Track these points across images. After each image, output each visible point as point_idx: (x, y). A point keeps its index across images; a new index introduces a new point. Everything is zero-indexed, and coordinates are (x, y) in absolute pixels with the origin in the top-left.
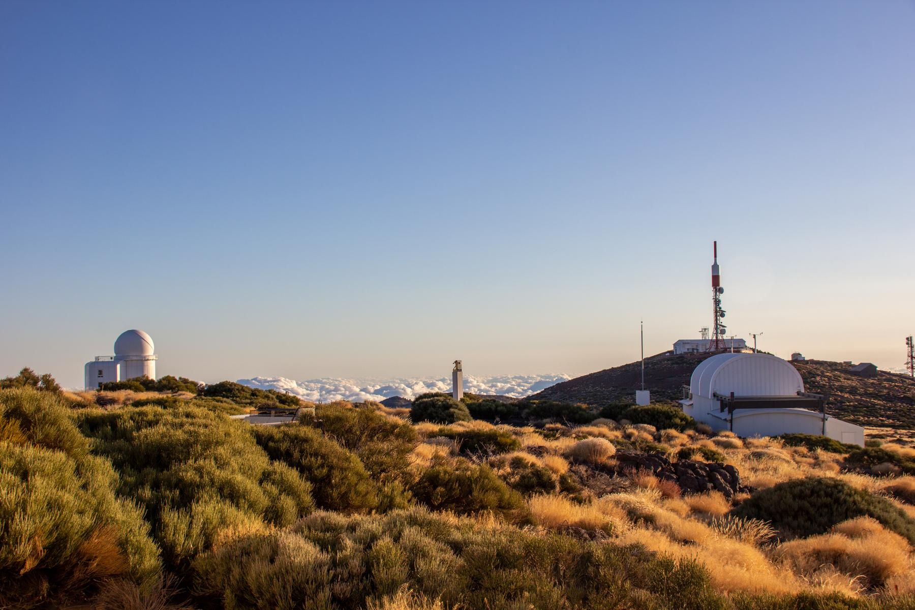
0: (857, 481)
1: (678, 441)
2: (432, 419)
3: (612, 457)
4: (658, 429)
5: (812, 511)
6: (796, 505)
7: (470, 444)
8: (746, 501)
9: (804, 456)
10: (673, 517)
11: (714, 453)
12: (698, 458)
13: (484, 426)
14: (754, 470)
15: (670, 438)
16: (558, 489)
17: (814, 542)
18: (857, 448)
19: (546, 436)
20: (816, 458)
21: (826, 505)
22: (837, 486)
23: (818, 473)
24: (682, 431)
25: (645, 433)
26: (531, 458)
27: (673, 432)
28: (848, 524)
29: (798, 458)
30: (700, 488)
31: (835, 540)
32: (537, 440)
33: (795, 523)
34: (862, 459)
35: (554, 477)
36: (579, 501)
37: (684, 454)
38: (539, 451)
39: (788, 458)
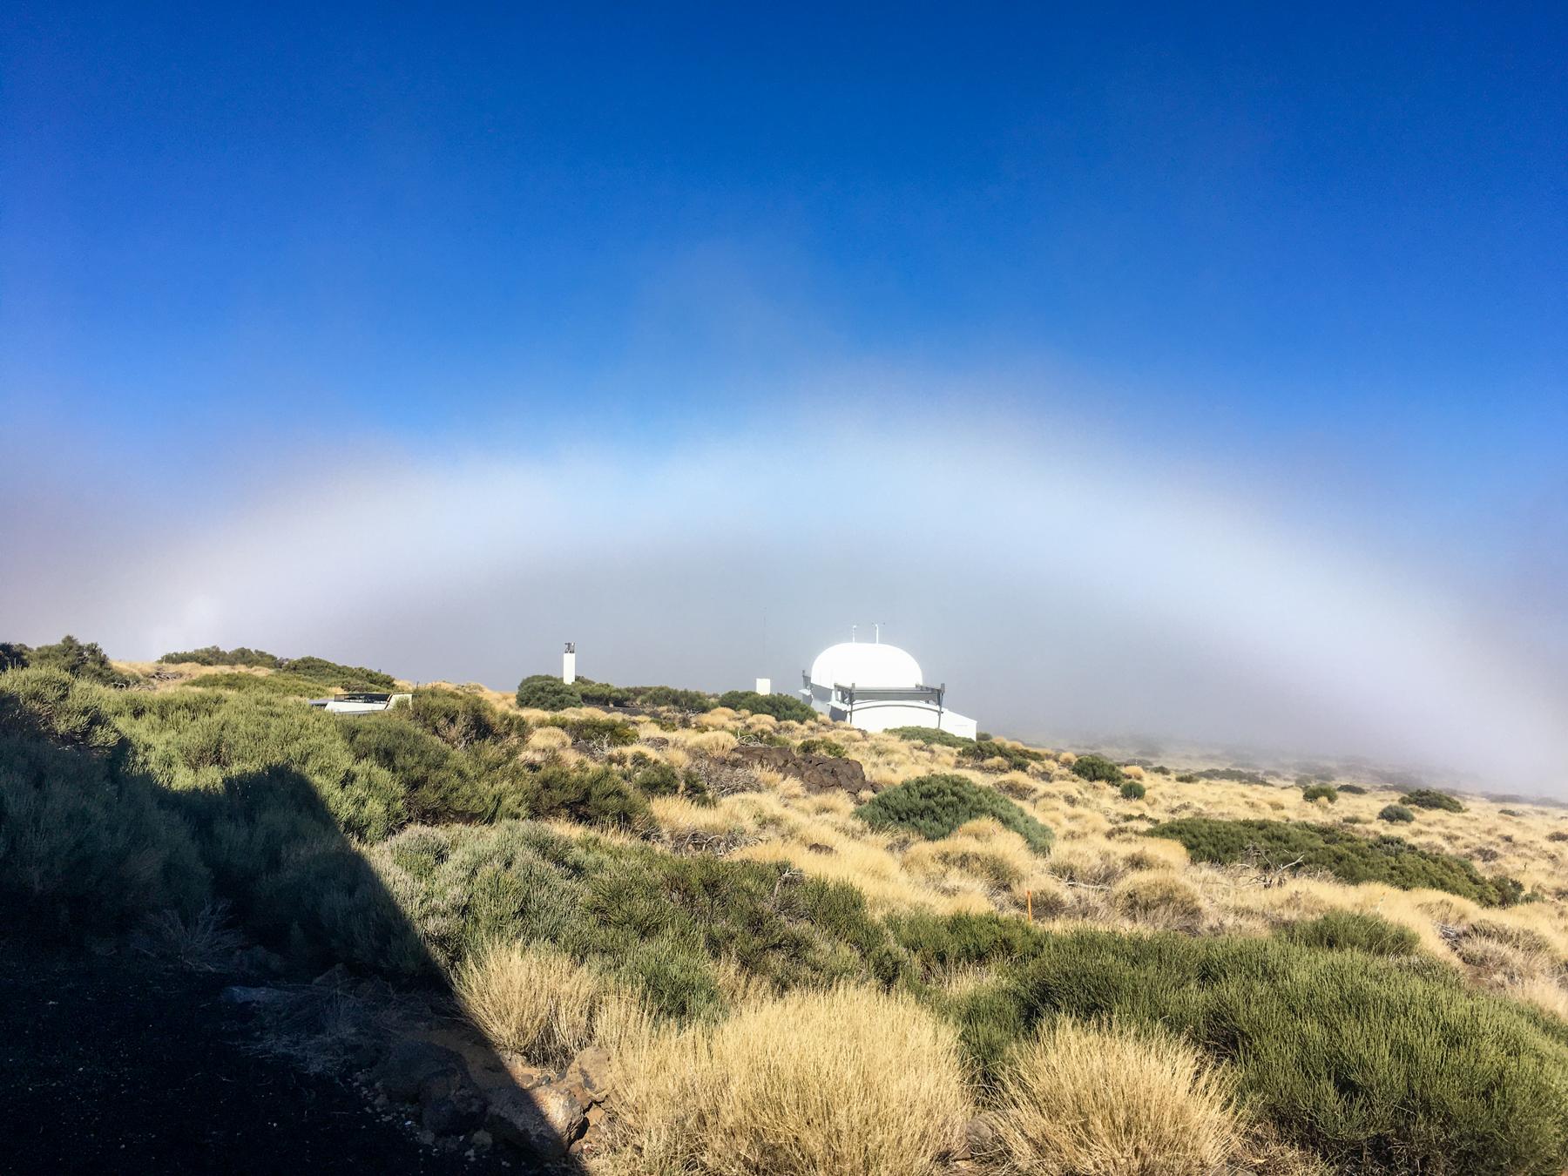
1: (797, 733)
2: (540, 704)
4: (778, 719)
5: (938, 810)
6: (922, 803)
7: (583, 734)
8: (872, 801)
9: (921, 749)
11: (837, 747)
12: (822, 752)
13: (599, 714)
14: (875, 765)
17: (942, 845)
18: (971, 741)
19: (663, 727)
20: (932, 752)
21: (952, 804)
22: (958, 782)
23: (938, 769)
24: (802, 722)
25: (766, 722)
26: (652, 754)
27: (793, 723)
28: (972, 825)
30: (823, 787)
31: (962, 842)
32: (655, 731)
33: (922, 823)
34: (978, 751)
35: (679, 772)
36: (704, 802)
37: (807, 748)
39: (907, 752)
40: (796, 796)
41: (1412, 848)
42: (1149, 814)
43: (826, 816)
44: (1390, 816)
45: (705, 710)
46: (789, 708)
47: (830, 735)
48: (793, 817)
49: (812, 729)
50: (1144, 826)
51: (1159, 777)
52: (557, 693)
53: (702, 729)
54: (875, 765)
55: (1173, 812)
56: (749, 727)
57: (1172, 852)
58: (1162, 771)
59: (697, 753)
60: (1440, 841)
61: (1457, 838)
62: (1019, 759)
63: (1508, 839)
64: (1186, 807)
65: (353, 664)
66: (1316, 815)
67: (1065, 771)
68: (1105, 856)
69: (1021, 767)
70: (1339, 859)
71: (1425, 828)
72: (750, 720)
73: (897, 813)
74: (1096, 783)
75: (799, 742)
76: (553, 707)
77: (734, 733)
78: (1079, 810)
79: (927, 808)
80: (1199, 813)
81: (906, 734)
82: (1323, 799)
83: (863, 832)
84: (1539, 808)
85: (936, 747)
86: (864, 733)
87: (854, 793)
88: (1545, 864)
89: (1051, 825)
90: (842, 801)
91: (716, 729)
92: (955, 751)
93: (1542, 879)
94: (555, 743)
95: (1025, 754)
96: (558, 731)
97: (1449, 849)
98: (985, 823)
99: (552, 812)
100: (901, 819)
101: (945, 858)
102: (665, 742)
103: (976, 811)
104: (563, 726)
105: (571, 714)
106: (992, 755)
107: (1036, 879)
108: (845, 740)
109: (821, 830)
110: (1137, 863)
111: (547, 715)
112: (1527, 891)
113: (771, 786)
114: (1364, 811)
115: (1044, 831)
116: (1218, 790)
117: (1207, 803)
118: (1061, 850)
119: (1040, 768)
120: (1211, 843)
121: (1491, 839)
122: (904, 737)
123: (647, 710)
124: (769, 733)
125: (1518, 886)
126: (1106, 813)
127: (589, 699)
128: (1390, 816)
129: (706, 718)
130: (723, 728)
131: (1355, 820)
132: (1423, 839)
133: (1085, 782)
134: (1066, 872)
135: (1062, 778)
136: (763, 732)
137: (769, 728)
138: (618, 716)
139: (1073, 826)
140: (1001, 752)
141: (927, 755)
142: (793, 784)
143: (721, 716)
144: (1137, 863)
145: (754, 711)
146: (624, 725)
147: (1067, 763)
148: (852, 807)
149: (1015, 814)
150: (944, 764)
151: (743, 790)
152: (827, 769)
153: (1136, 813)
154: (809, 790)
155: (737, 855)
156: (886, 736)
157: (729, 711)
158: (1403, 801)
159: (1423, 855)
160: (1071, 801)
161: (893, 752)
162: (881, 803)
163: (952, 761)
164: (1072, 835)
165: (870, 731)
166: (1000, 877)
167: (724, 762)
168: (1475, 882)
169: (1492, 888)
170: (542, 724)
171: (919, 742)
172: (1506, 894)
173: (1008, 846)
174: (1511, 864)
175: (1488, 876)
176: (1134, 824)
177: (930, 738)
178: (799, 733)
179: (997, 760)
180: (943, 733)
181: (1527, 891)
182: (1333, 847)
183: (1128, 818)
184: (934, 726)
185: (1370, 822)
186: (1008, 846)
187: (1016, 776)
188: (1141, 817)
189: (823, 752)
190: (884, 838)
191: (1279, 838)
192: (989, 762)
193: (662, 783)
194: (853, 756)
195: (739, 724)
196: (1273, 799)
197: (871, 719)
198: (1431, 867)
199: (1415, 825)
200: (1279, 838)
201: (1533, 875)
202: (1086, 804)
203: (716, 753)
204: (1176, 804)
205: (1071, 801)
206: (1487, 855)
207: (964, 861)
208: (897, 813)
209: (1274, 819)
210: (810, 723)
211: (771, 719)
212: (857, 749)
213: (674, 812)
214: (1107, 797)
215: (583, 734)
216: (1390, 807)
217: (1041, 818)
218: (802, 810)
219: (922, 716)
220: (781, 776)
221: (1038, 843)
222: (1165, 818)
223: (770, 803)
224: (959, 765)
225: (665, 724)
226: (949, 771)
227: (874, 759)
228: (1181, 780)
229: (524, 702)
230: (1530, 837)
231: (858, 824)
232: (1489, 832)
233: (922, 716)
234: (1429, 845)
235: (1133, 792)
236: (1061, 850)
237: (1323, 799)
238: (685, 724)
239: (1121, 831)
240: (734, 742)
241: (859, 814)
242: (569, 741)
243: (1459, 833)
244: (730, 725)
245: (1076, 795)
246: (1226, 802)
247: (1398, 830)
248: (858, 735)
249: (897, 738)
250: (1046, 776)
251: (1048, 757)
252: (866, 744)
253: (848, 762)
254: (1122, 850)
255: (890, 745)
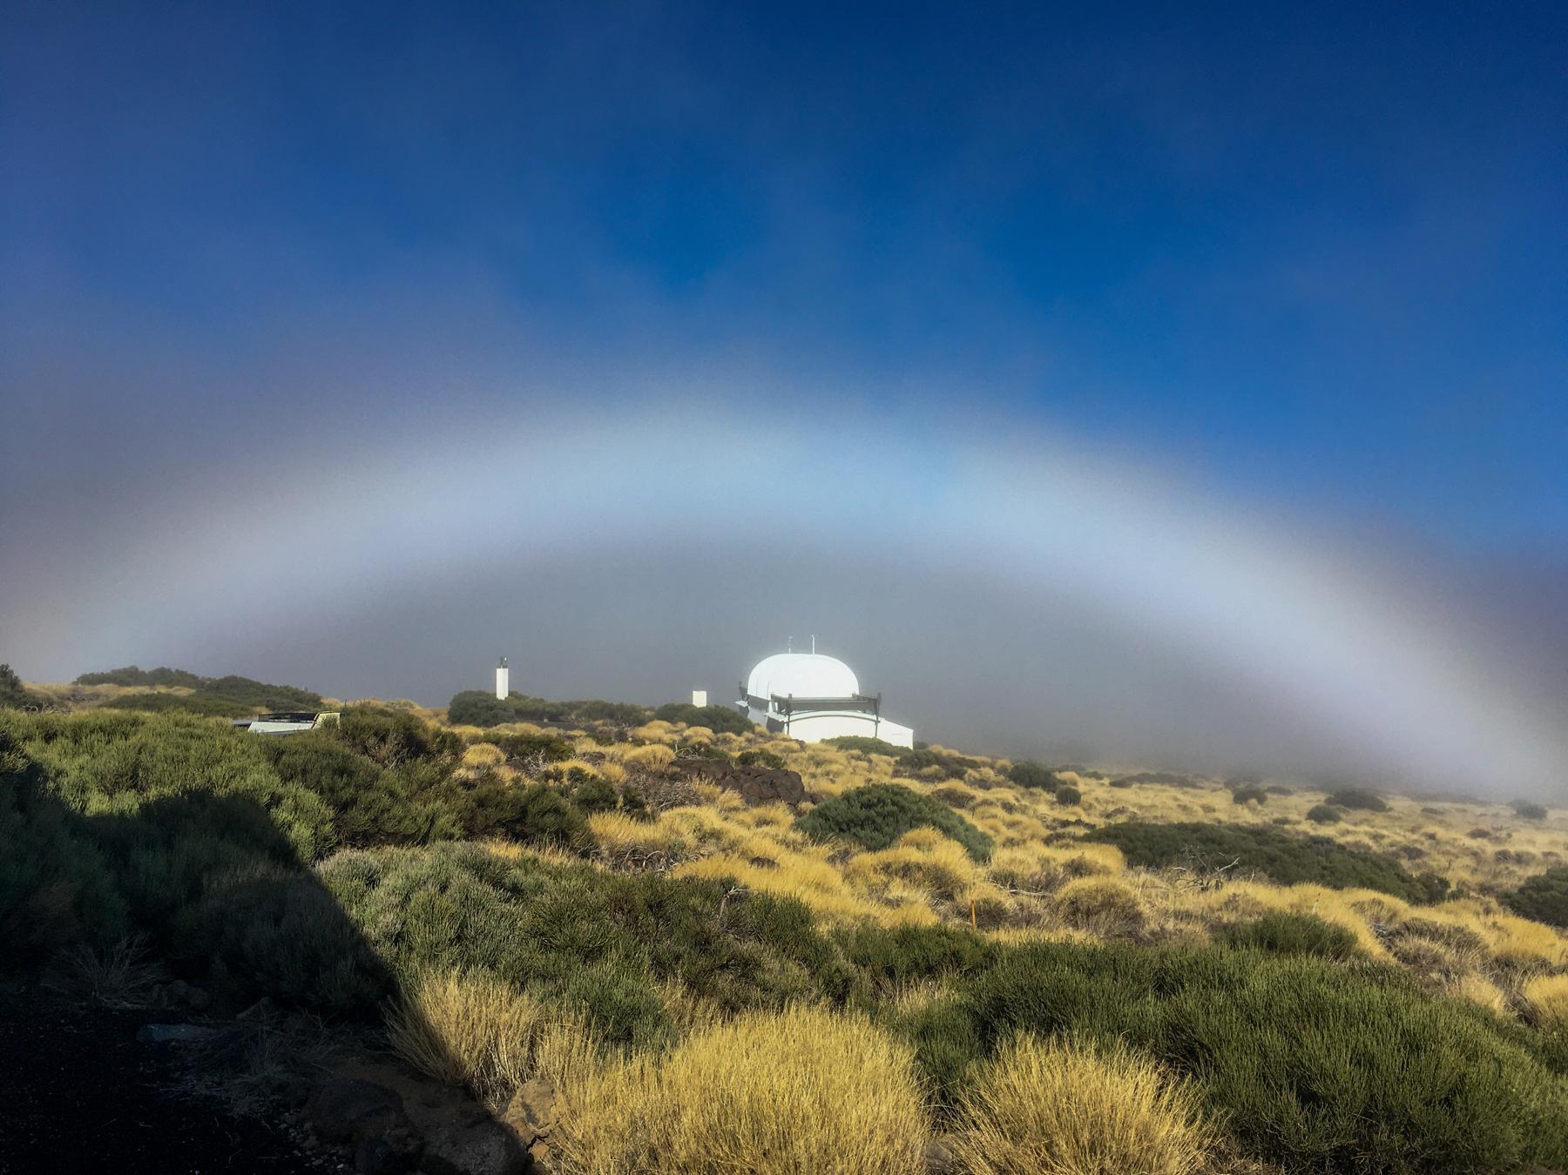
0: (915, 786)
2: (473, 720)
3: (672, 763)
4: (715, 732)
6: (863, 813)
7: (518, 750)
8: (812, 812)
9: (858, 758)
10: (742, 832)
11: (775, 758)
12: (760, 764)
14: (813, 776)
15: (726, 741)
16: (621, 799)
17: (884, 856)
18: (907, 749)
19: (600, 742)
20: (870, 761)
21: (891, 814)
24: (739, 734)
25: (703, 734)
28: (912, 834)
29: (853, 762)
31: (903, 852)
32: (591, 746)
33: (862, 833)
34: (913, 761)
35: (616, 787)
36: (644, 818)
37: (746, 759)
38: (597, 758)
40: (736, 809)
41: (1342, 848)
42: (1085, 818)
43: (765, 829)
44: (1318, 816)
45: (641, 723)
46: (726, 720)
47: (768, 746)
48: (734, 830)
49: (749, 740)
50: (1081, 831)
51: (1094, 782)
52: (491, 708)
53: (639, 742)
54: (813, 776)
55: (1108, 816)
56: (686, 740)
57: (1107, 857)
58: (1097, 776)
59: (634, 767)
60: (1367, 841)
61: (1383, 837)
62: (956, 767)
63: (1432, 837)
64: (1121, 811)
65: (277, 683)
66: (1247, 816)
67: (1002, 777)
68: (1045, 862)
69: (959, 775)
70: (1272, 860)
71: (1351, 828)
72: (687, 733)
73: (838, 823)
74: (1034, 790)
75: (737, 754)
76: (486, 723)
77: (672, 746)
78: (1017, 817)
79: (868, 818)
80: (1134, 816)
81: (844, 744)
82: (1253, 801)
83: (804, 844)
84: (1459, 806)
85: (874, 756)
86: (801, 743)
87: (793, 805)
88: (1467, 861)
89: (991, 833)
90: (781, 813)
91: (653, 742)
92: (892, 760)
93: (1466, 875)
94: (489, 759)
95: (962, 762)
96: (491, 747)
97: (1375, 847)
98: (926, 833)
99: (488, 831)
100: (841, 830)
101: (886, 868)
102: (602, 756)
103: (917, 821)
104: (496, 742)
105: (504, 730)
106: (929, 763)
107: (979, 887)
108: (783, 751)
109: (761, 842)
110: (1077, 869)
111: (480, 732)
112: (1453, 887)
113: (710, 800)
114: (1294, 812)
115: (985, 839)
116: (1151, 794)
117: (1141, 807)
118: (1001, 857)
119: (977, 775)
120: (1147, 846)
121: (1415, 837)
122: (841, 747)
123: (583, 725)
124: (706, 746)
125: (1445, 883)
126: (1042, 818)
127: (523, 714)
128: (1318, 816)
129: (643, 732)
130: (660, 741)
131: (1286, 821)
132: (1349, 839)
133: (1022, 789)
134: (1006, 879)
135: (999, 785)
136: (700, 744)
137: (706, 741)
138: (553, 732)
139: (1012, 833)
140: (938, 759)
141: (865, 764)
142: (732, 797)
143: (658, 729)
144: (1077, 869)
145: (691, 724)
146: (560, 740)
147: (1002, 770)
148: (791, 818)
149: (956, 822)
150: (883, 774)
151: (682, 804)
152: (765, 779)
153: (1073, 819)
154: (748, 802)
155: (679, 872)
156: (823, 746)
157: (666, 724)
158: (1329, 801)
159: (1351, 854)
160: (1009, 808)
161: (830, 762)
162: (822, 814)
163: (890, 770)
164: (1010, 843)
165: (808, 741)
166: (943, 886)
167: (661, 776)
168: (1403, 880)
169: (1419, 886)
170: (475, 740)
171: (856, 752)
172: (1432, 891)
173: (950, 855)
174: (1436, 862)
175: (1415, 874)
176: (1071, 829)
177: (868, 747)
178: (736, 745)
179: (935, 767)
180: (881, 742)
181: (1453, 887)
182: (1266, 848)
183: (1066, 824)
184: (871, 736)
185: (1299, 823)
186: (950, 855)
187: (954, 784)
188: (1078, 823)
189: (761, 764)
190: (825, 850)
191: (1213, 841)
192: (926, 771)
193: (600, 798)
194: (793, 768)
195: (677, 737)
196: (1203, 801)
197: (808, 730)
198: (1360, 866)
199: (1342, 825)
200: (1213, 841)
201: (1459, 872)
202: (1024, 810)
203: (654, 767)
204: (1111, 808)
205: (1009, 808)
206: (1413, 853)
207: (906, 871)
208: (838, 823)
209: (1207, 821)
210: (748, 734)
211: (708, 731)
212: (795, 761)
213: (614, 828)
214: (1044, 806)
215: (518, 750)
216: (1317, 808)
217: (981, 827)
218: (742, 823)
219: (859, 726)
220: (719, 789)
221: (978, 851)
222: (1101, 823)
223: (710, 817)
224: (896, 774)
225: (603, 739)
226: (887, 780)
227: (812, 769)
228: (1113, 784)
229: (457, 717)
230: (1453, 834)
231: (798, 836)
232: (1413, 831)
233: (859, 726)
234: (1357, 844)
235: (1069, 797)
236: (1001, 857)
237: (1253, 801)
238: (622, 738)
239: (1059, 837)
240: (671, 755)
241: (797, 826)
242: (504, 757)
243: (1385, 832)
244: (667, 738)
245: (1013, 801)
246: (1160, 804)
247: (1326, 831)
248: (796, 746)
249: (835, 748)
250: (984, 784)
251: (984, 764)
252: (804, 755)
253: (787, 773)
254: (1061, 856)
255: (828, 756)
